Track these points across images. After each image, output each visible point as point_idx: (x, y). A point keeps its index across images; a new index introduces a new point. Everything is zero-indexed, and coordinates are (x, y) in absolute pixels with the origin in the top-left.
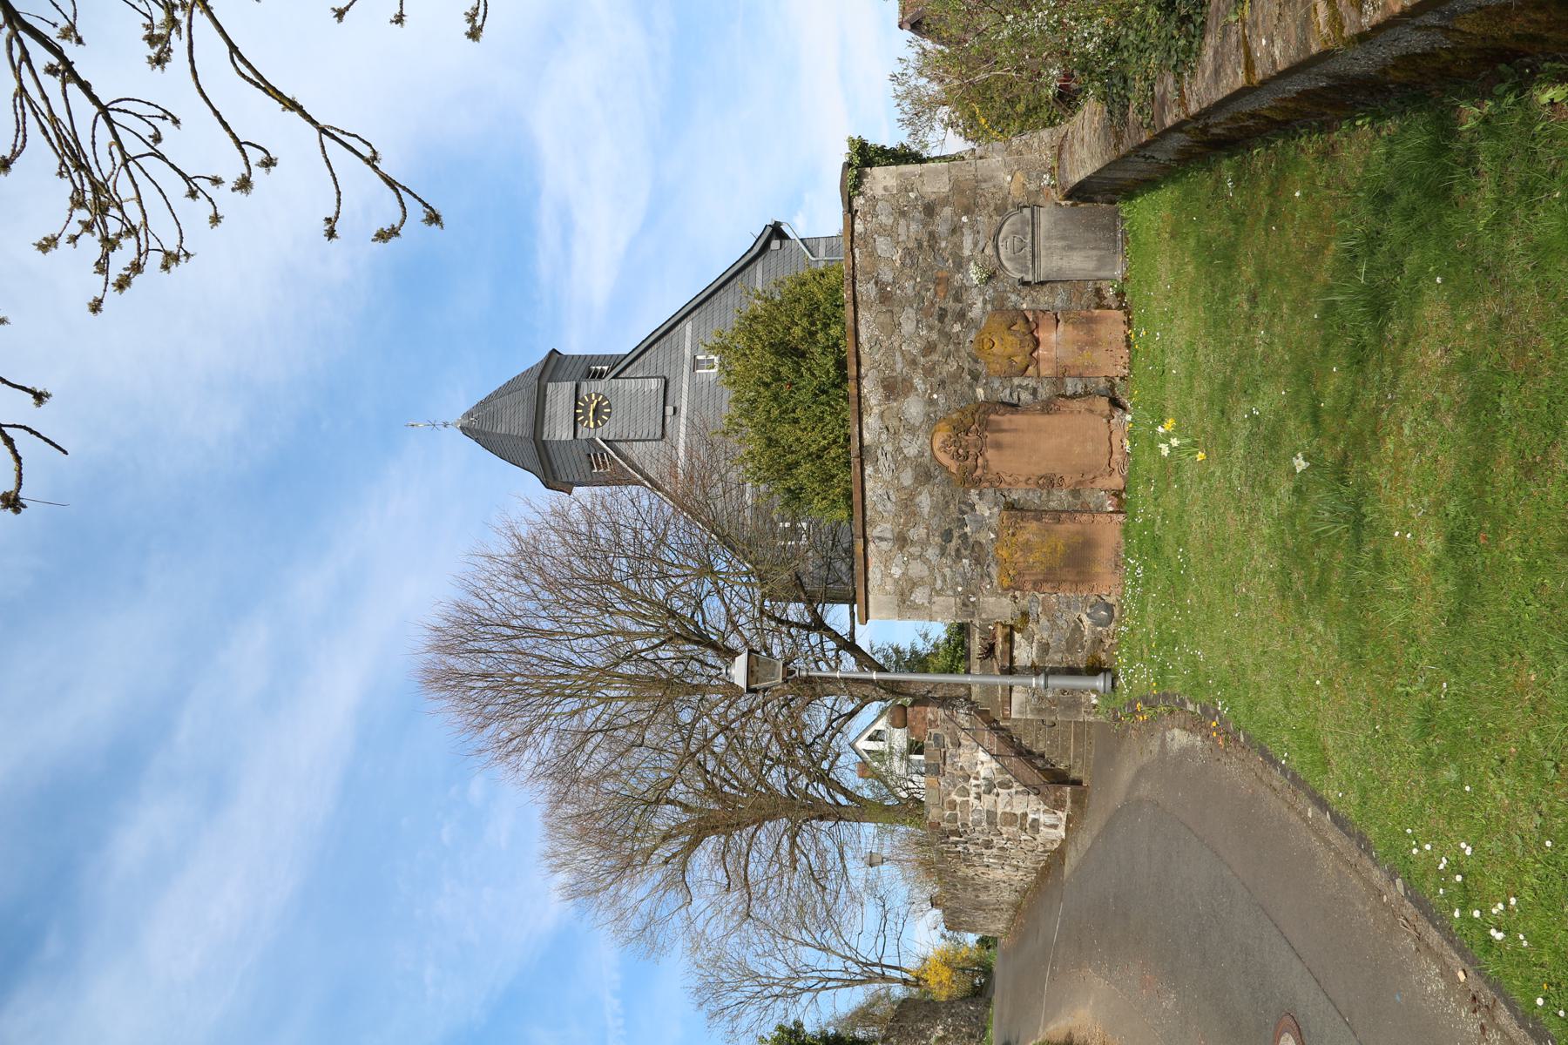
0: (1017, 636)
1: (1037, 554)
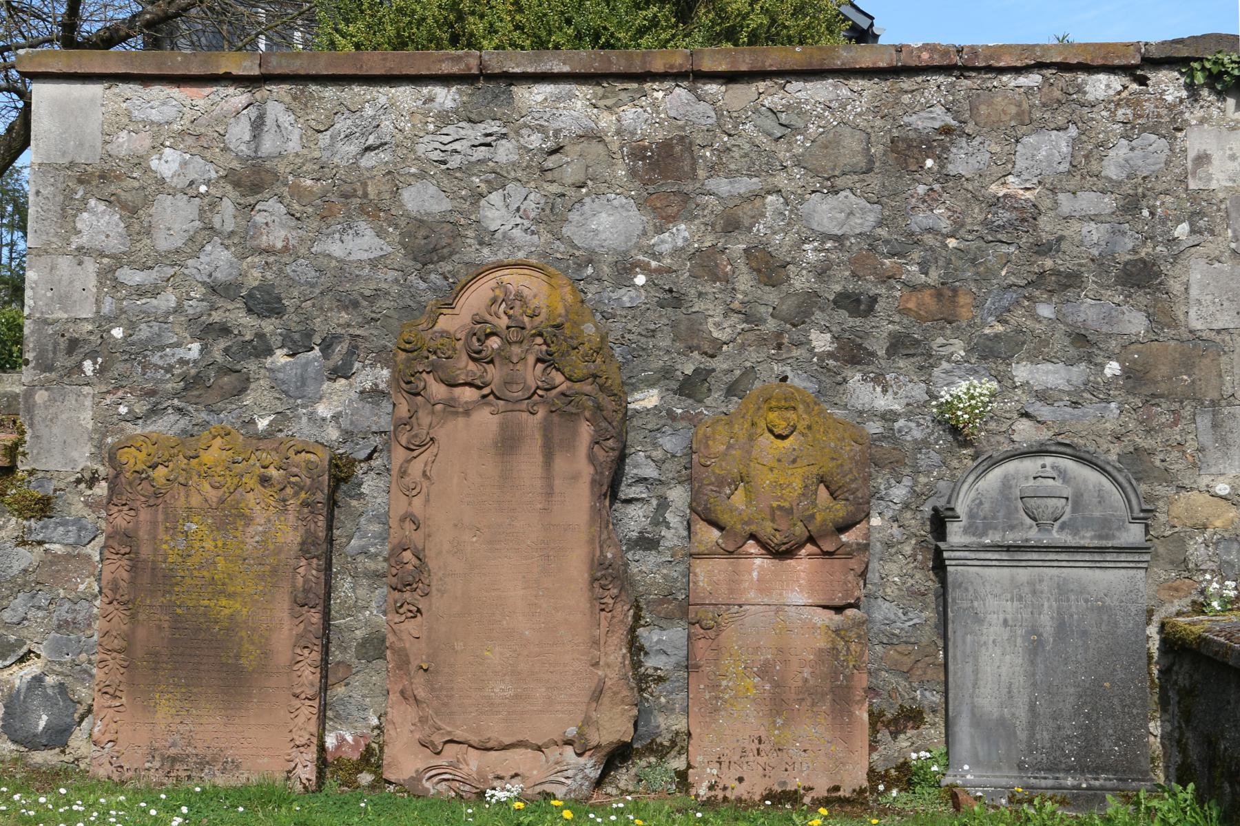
1: (209, 544)
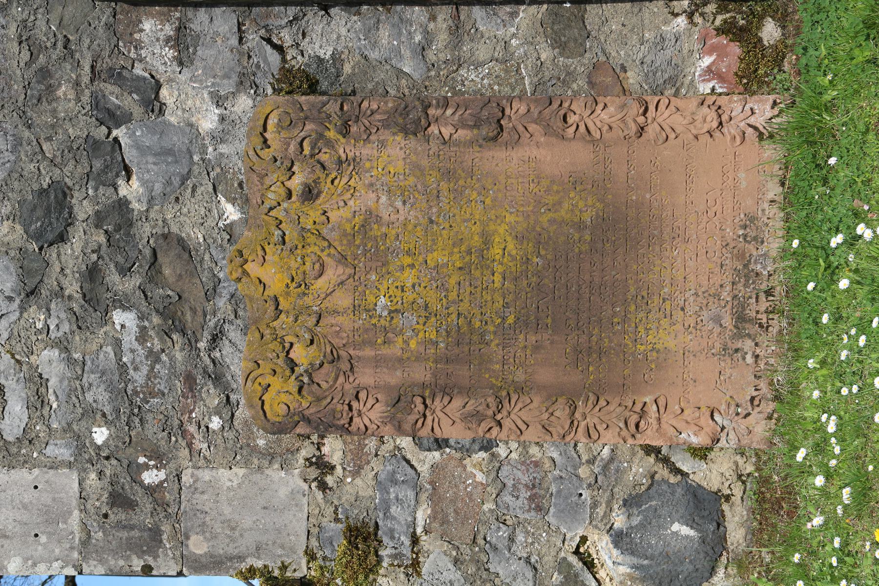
1: (409, 278)
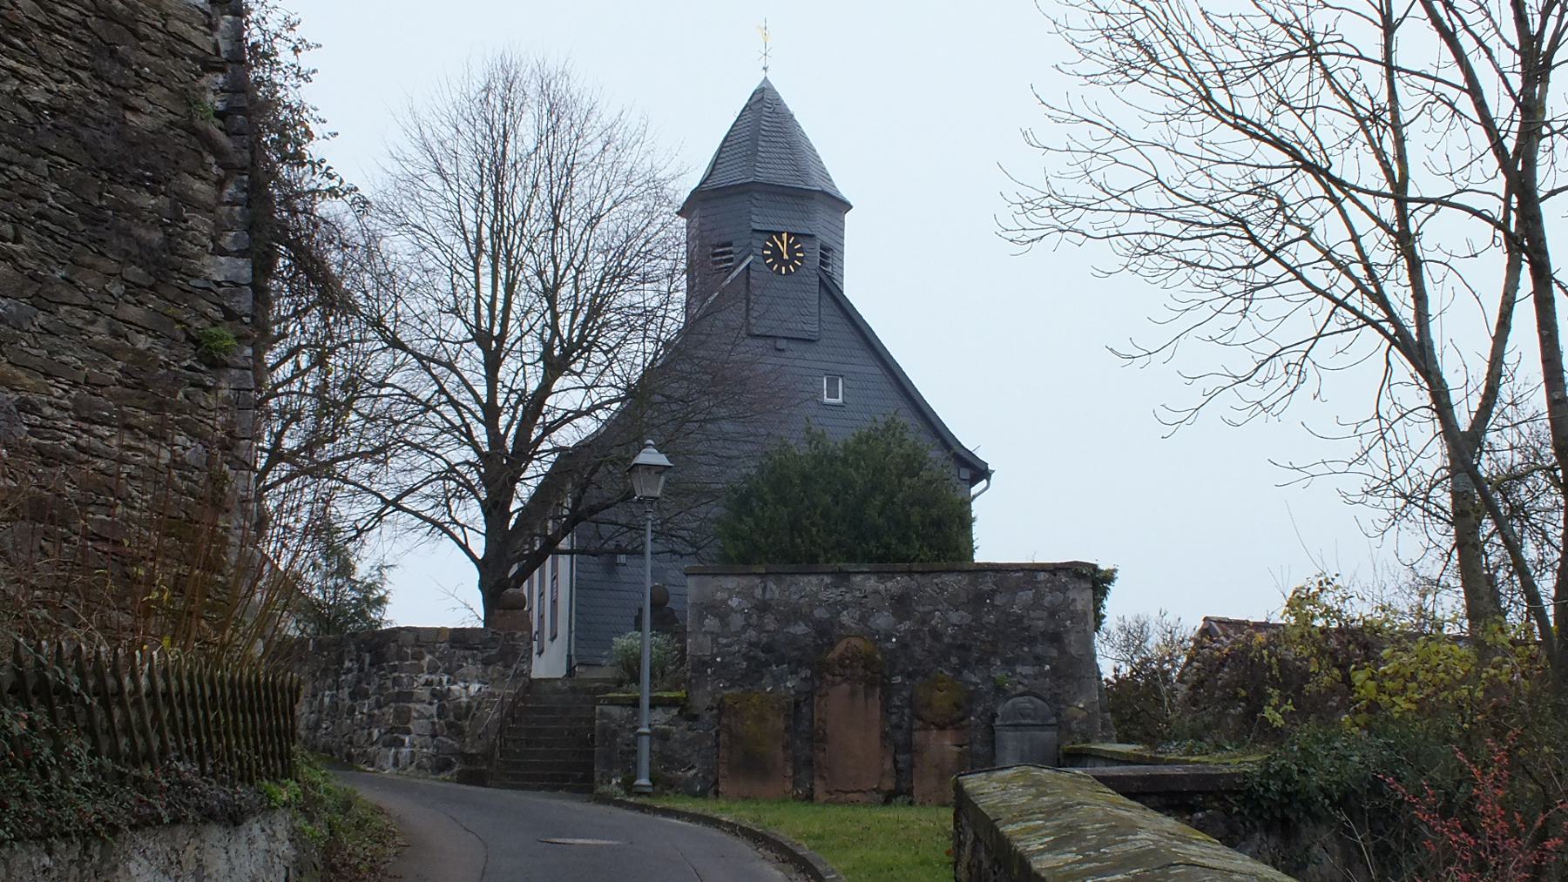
0: (675, 711)
